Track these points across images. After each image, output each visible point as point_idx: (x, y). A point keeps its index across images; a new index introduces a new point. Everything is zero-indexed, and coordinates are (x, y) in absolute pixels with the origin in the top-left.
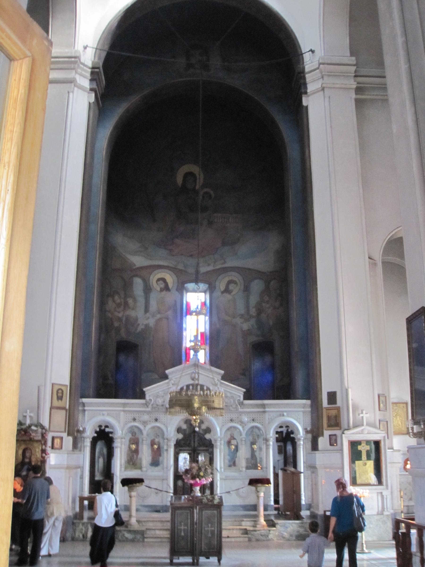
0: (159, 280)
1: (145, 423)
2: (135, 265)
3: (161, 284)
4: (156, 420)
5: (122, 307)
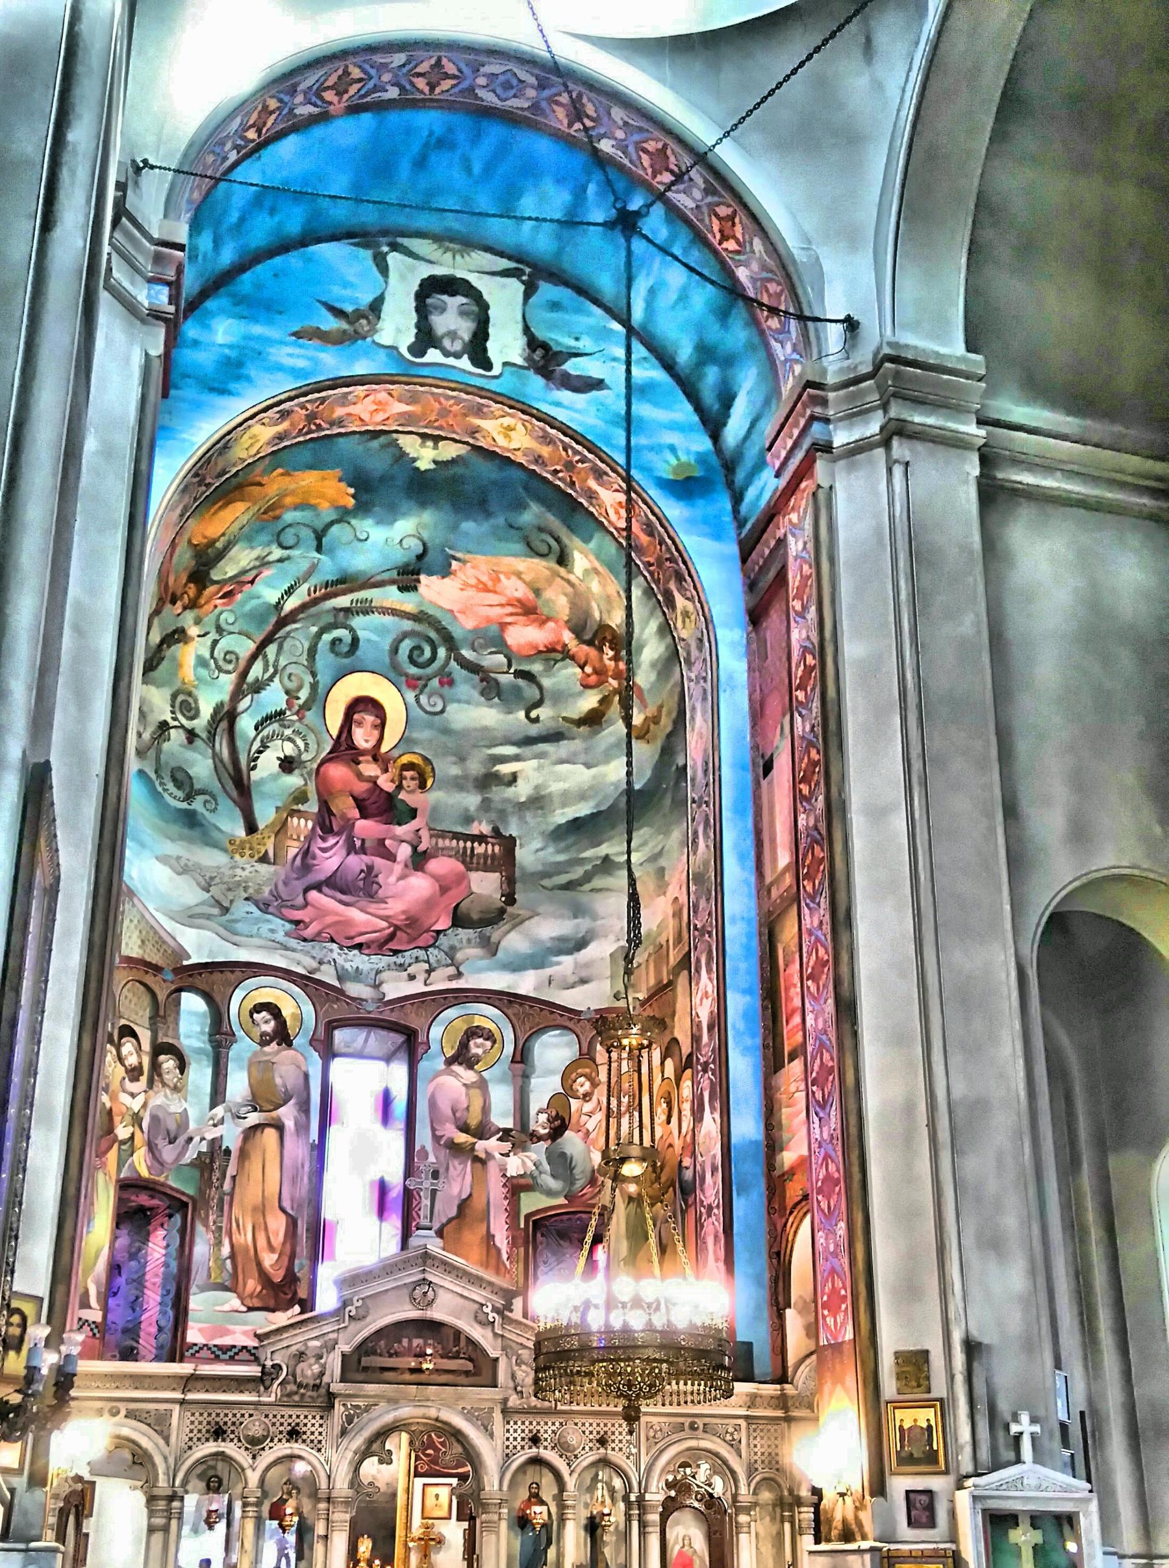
0: (259, 1008)
1: (255, 1444)
2: (189, 957)
3: (266, 1022)
4: (294, 1434)
5: (144, 1079)
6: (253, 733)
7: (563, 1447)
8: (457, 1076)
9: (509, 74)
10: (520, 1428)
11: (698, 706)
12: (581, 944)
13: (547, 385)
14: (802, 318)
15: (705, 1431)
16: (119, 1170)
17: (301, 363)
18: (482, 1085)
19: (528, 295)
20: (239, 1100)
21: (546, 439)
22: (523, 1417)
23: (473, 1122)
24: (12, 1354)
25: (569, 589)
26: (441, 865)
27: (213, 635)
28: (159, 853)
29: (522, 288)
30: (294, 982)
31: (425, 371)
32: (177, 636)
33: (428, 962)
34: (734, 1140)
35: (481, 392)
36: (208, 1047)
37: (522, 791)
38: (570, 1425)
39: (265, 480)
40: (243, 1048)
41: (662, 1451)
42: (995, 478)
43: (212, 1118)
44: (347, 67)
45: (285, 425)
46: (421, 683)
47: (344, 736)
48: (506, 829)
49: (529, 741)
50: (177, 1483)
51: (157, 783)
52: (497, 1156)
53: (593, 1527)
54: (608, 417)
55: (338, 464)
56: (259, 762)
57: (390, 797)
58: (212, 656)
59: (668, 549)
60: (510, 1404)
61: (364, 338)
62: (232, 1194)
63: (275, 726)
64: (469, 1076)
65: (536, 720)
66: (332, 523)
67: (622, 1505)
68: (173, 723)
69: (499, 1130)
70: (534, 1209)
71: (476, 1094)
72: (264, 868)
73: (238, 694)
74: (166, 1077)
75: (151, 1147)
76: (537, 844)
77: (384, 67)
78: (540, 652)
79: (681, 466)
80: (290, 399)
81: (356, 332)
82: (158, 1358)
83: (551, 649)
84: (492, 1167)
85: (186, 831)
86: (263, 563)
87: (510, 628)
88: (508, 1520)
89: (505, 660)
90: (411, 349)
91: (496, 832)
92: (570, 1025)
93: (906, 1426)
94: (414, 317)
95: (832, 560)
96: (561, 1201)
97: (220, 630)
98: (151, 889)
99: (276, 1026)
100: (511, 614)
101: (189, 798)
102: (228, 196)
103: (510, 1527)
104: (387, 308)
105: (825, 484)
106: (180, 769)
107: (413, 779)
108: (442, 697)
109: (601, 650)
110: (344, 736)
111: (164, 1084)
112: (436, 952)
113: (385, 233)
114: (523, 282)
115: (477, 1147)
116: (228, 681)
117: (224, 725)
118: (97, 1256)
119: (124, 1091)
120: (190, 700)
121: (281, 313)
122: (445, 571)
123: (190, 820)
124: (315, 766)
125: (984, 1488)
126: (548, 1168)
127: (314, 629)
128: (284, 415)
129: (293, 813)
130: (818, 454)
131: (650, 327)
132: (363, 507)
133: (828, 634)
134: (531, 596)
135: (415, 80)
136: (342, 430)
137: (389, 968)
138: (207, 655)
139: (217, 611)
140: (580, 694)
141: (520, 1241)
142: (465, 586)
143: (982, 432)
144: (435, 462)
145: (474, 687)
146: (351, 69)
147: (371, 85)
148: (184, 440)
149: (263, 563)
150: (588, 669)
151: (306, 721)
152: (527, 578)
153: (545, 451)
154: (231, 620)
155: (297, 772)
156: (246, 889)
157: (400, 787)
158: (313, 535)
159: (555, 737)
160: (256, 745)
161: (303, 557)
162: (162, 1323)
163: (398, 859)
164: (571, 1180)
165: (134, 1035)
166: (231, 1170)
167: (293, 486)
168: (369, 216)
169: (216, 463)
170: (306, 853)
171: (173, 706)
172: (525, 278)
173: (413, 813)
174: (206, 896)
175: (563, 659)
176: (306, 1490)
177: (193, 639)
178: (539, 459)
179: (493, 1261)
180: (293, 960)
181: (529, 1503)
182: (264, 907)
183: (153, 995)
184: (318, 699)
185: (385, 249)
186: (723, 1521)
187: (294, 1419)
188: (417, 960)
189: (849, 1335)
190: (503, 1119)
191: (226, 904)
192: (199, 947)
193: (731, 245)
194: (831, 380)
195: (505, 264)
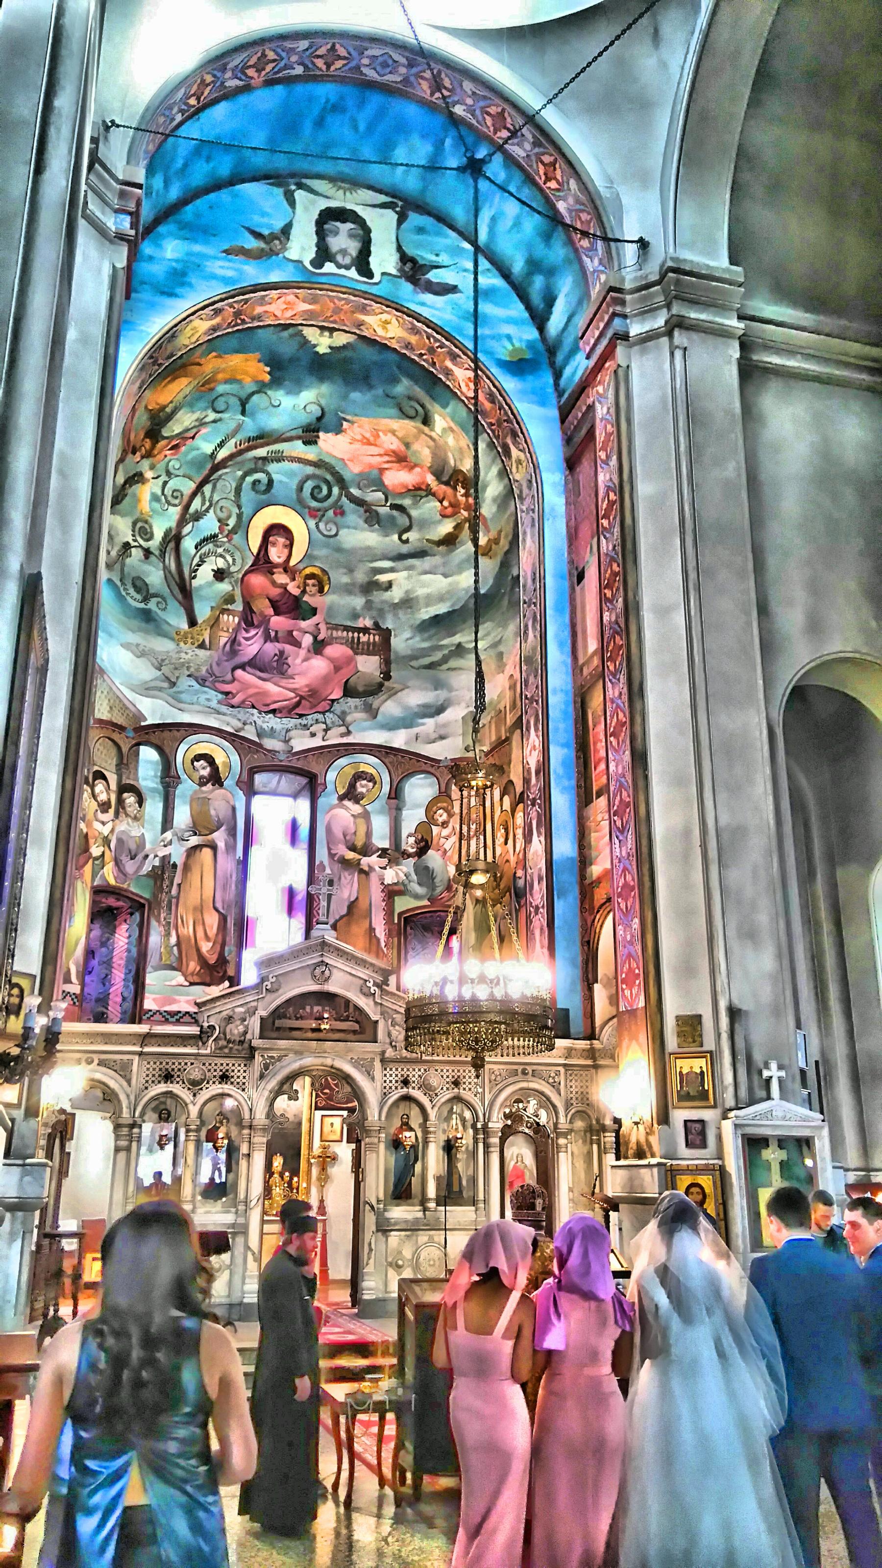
0: (198, 757)
1: (195, 1085)
2: (145, 719)
4: (224, 1078)
5: (112, 811)
6: (193, 551)
7: (426, 1088)
8: (347, 808)
9: (386, 57)
10: (395, 1074)
11: (528, 531)
12: (440, 710)
14: (606, 239)
15: (533, 1076)
16: (93, 880)
17: (230, 273)
18: (366, 815)
19: (400, 222)
20: (183, 827)
21: (414, 331)
22: (397, 1065)
23: (359, 843)
24: (13, 1017)
25: (431, 443)
26: (335, 650)
27: (164, 478)
28: (123, 641)
29: (396, 217)
30: (224, 738)
31: (323, 279)
32: (136, 478)
33: (325, 723)
34: (555, 857)
35: (365, 295)
36: (160, 787)
37: (396, 595)
38: (432, 1071)
39: (202, 361)
40: (186, 788)
41: (501, 1091)
43: (163, 841)
45: (218, 320)
46: (320, 513)
47: (262, 553)
49: (401, 557)
50: (137, 1114)
52: (377, 869)
53: (449, 1147)
55: (257, 349)
56: (198, 573)
57: (297, 600)
58: (163, 493)
59: (506, 413)
60: (387, 1055)
61: (277, 254)
63: (210, 546)
64: (356, 809)
65: (407, 541)
66: (253, 393)
67: (471, 1131)
68: (133, 544)
69: (379, 849)
70: (405, 909)
71: (361, 822)
72: (202, 653)
73: (182, 521)
74: (128, 809)
75: (117, 862)
76: (407, 634)
77: (292, 51)
78: (409, 490)
79: (515, 350)
80: (222, 300)
81: (271, 250)
82: (122, 1021)
83: (417, 488)
84: (374, 877)
85: (143, 625)
86: (201, 423)
87: (387, 472)
89: (383, 497)
90: (312, 263)
91: (377, 625)
92: (432, 770)
93: (685, 1071)
94: (315, 239)
96: (425, 902)
97: (169, 474)
98: (117, 669)
99: (211, 771)
100: (388, 462)
101: (146, 600)
102: (175, 147)
103: (387, 1148)
104: (294, 232)
105: (624, 364)
106: (139, 578)
107: (314, 585)
108: (336, 524)
109: (455, 489)
110: (262, 553)
111: (127, 815)
112: (331, 715)
113: (293, 175)
114: (397, 212)
115: (362, 862)
116: (174, 512)
117: (172, 545)
118: (76, 944)
119: (97, 820)
120: (147, 526)
121: (214, 235)
122: (338, 430)
123: (147, 616)
124: (240, 576)
125: (743, 1118)
126: (414, 877)
127: (240, 473)
128: (217, 312)
129: (224, 611)
131: (492, 246)
132: (276, 382)
134: (403, 448)
135: (315, 60)
136: (261, 324)
137: (296, 727)
138: (159, 492)
139: (167, 459)
140: (440, 522)
141: (395, 933)
142: (353, 441)
143: (742, 325)
144: (330, 347)
145: (360, 517)
146: (268, 52)
147: (282, 64)
148: (142, 331)
149: (201, 423)
150: (446, 503)
151: (233, 542)
152: (400, 434)
153: (413, 339)
154: (177, 466)
155: (226, 580)
156: (188, 668)
157: (304, 592)
159: (421, 554)
160: (196, 560)
161: (232, 419)
162: (126, 994)
163: (303, 646)
164: (433, 887)
165: (104, 778)
166: (177, 880)
167: (223, 366)
168: (281, 163)
170: (234, 641)
171: (133, 531)
172: (398, 209)
173: (314, 611)
174: (159, 673)
175: (427, 496)
176: (233, 1120)
177: (148, 480)
178: (408, 346)
179: (374, 948)
180: (223, 721)
182: (202, 682)
184: (243, 526)
185: (293, 187)
186: (547, 1143)
187: (225, 1067)
188: (317, 721)
189: (642, 1004)
190: (381, 841)
192: (153, 712)
193: (553, 184)
194: (628, 286)
195: (383, 198)
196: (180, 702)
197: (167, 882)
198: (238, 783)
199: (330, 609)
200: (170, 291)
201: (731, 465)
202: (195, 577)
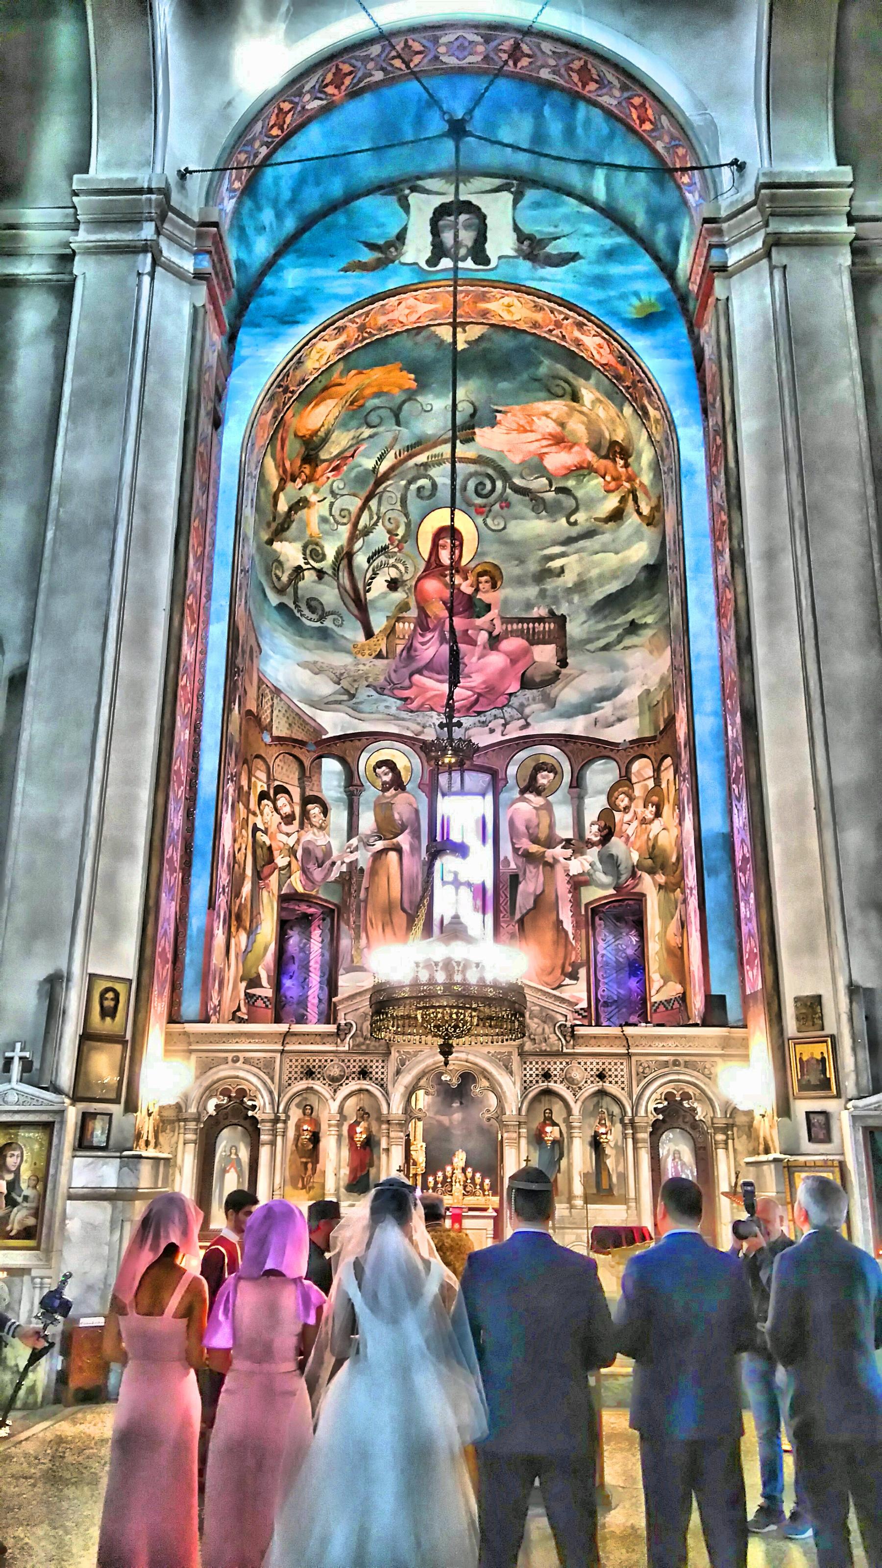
0: (380, 764)
1: (336, 1081)
2: (327, 733)
3: (386, 774)
4: (364, 1074)
5: (296, 823)
6: (366, 565)
7: (569, 1081)
9: (460, 40)
10: (534, 1068)
11: (669, 491)
13: (534, 267)
15: (686, 1067)
16: (280, 889)
17: (348, 290)
18: (548, 807)
19: (515, 202)
21: (538, 308)
22: (537, 1059)
23: (543, 834)
24: (108, 1019)
25: (585, 419)
26: (512, 644)
27: (330, 499)
30: (405, 743)
32: (301, 504)
33: (504, 718)
37: (569, 579)
38: (575, 1064)
39: (343, 381)
40: (370, 794)
42: (875, 264)
43: (349, 847)
44: (337, 66)
46: (487, 509)
48: (558, 608)
49: (569, 541)
50: (281, 1110)
51: (296, 611)
53: (597, 1144)
54: (583, 280)
57: (470, 598)
58: (331, 514)
59: (638, 373)
61: (393, 261)
62: (366, 901)
63: (382, 558)
64: (538, 801)
65: (575, 523)
66: (404, 402)
67: (619, 1126)
68: (305, 567)
69: (563, 840)
70: (592, 899)
71: (543, 813)
73: (352, 538)
74: (314, 820)
75: (305, 871)
76: (583, 617)
77: (367, 59)
79: (643, 306)
80: (342, 318)
81: (387, 258)
82: (319, 1022)
83: (579, 468)
84: (559, 869)
85: (321, 643)
88: (528, 1138)
90: (428, 262)
91: (551, 612)
92: (611, 754)
93: (805, 1058)
94: (430, 238)
95: (730, 357)
96: (612, 891)
97: (333, 493)
98: (294, 687)
101: (322, 618)
102: (277, 179)
103: (529, 1143)
104: (409, 236)
105: (723, 297)
108: (503, 517)
109: (614, 461)
111: (312, 825)
112: (509, 710)
116: (345, 531)
117: (345, 562)
118: (266, 949)
120: (318, 548)
121: (332, 256)
122: (493, 423)
123: (324, 634)
124: (414, 583)
125: (865, 1108)
126: (599, 866)
127: (403, 483)
128: (341, 330)
129: (398, 619)
130: (716, 274)
131: (613, 204)
132: (423, 386)
133: (728, 416)
134: (559, 429)
135: (393, 62)
136: (389, 333)
139: (330, 481)
140: (605, 498)
141: (583, 924)
142: (509, 431)
143: (852, 229)
145: (526, 506)
146: (341, 66)
147: (360, 74)
148: (266, 363)
150: (608, 478)
152: (554, 415)
156: (367, 679)
157: (477, 590)
158: (392, 415)
159: (590, 534)
160: (368, 575)
164: (618, 875)
165: (287, 792)
166: (365, 884)
167: (367, 381)
169: (294, 375)
170: (410, 648)
171: (304, 554)
173: (488, 608)
174: (338, 687)
176: (373, 1115)
178: (535, 325)
179: (563, 941)
181: (544, 1124)
182: (381, 691)
183: (301, 764)
184: (412, 533)
185: (407, 191)
186: (706, 1138)
188: (496, 717)
189: (760, 986)
190: (565, 831)
191: (352, 692)
192: (335, 725)
193: (647, 126)
194: (723, 214)
195: (497, 182)
196: (360, 712)
197: (355, 887)
198: (419, 786)
199: (506, 602)
200: (291, 319)
201: (845, 382)
202: (369, 590)
